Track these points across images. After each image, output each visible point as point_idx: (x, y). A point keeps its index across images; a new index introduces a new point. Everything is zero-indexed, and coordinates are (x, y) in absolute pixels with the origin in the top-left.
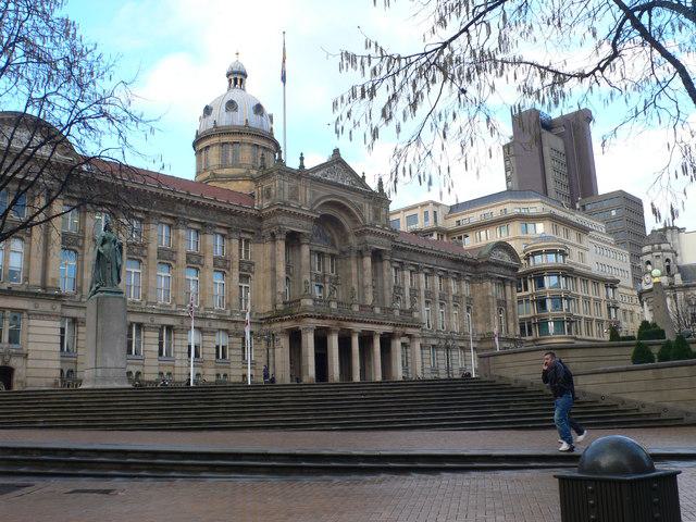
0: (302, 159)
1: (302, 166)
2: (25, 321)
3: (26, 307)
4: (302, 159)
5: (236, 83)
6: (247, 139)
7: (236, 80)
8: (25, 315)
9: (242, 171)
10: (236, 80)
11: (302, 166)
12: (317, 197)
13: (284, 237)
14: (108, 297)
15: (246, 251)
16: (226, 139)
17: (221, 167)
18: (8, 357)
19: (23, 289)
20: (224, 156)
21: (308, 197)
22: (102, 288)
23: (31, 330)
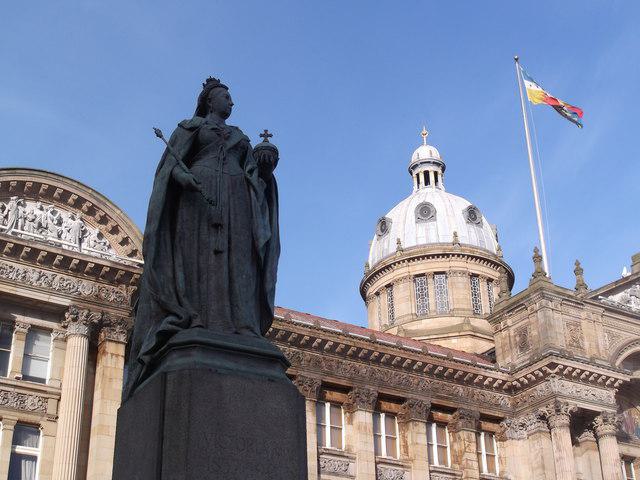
0: (578, 271)
1: (581, 285)
4: (578, 271)
5: (427, 182)
6: (458, 264)
7: (426, 174)
9: (456, 321)
10: (426, 174)
11: (581, 285)
12: (620, 343)
13: (566, 420)
14: (211, 371)
15: (490, 457)
16: (420, 267)
17: (422, 313)
20: (422, 295)
21: (601, 342)
22: (182, 336)
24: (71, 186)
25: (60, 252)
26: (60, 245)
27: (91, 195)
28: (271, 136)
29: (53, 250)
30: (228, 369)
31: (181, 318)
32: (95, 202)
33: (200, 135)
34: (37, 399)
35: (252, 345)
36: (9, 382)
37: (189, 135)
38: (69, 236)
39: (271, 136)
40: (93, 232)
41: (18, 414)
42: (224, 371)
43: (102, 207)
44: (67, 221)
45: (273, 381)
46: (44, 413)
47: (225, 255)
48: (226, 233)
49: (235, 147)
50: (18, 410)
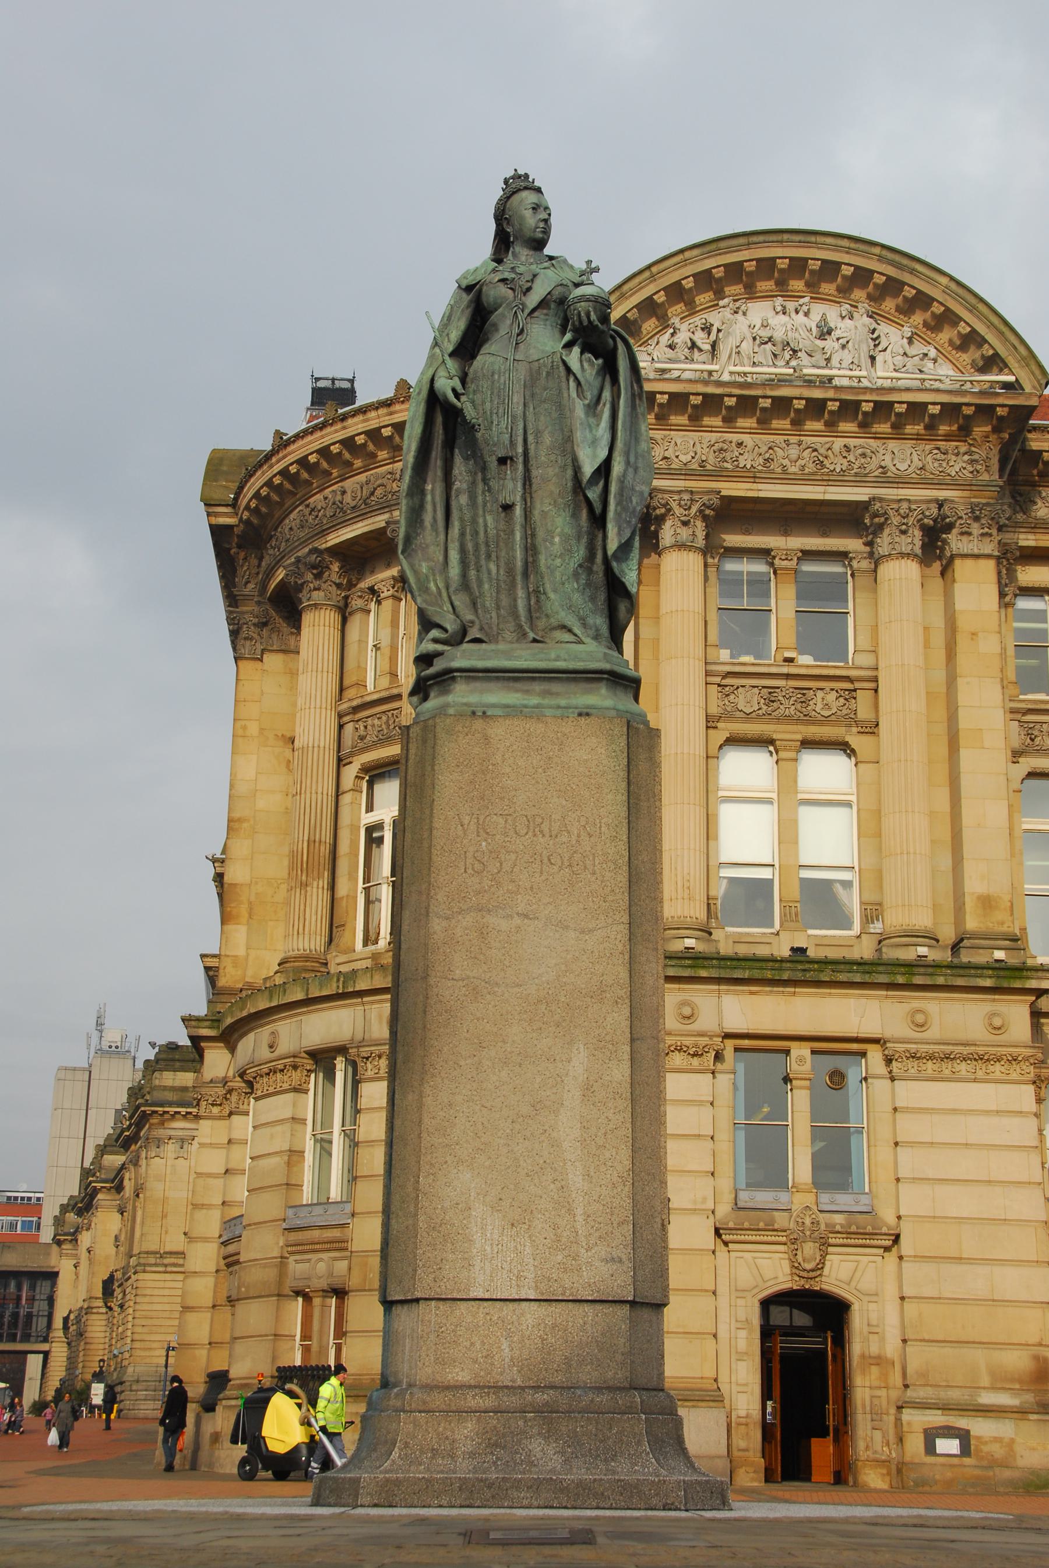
2: (881, 1087)
3: (870, 1028)
8: (875, 1055)
18: (809, 1249)
19: (865, 951)
23: (909, 1127)
24: (837, 248)
25: (830, 394)
26: (830, 379)
27: (881, 259)
28: (597, 270)
29: (817, 394)
30: (507, 706)
31: (446, 631)
32: (891, 271)
33: (484, 299)
34: (834, 694)
35: (556, 660)
36: (774, 670)
37: (466, 298)
38: (847, 356)
39: (597, 270)
40: (893, 336)
41: (801, 728)
42: (498, 712)
43: (906, 277)
44: (843, 328)
45: (588, 714)
46: (851, 720)
47: (518, 511)
48: (521, 467)
49: (543, 304)
50: (798, 721)
